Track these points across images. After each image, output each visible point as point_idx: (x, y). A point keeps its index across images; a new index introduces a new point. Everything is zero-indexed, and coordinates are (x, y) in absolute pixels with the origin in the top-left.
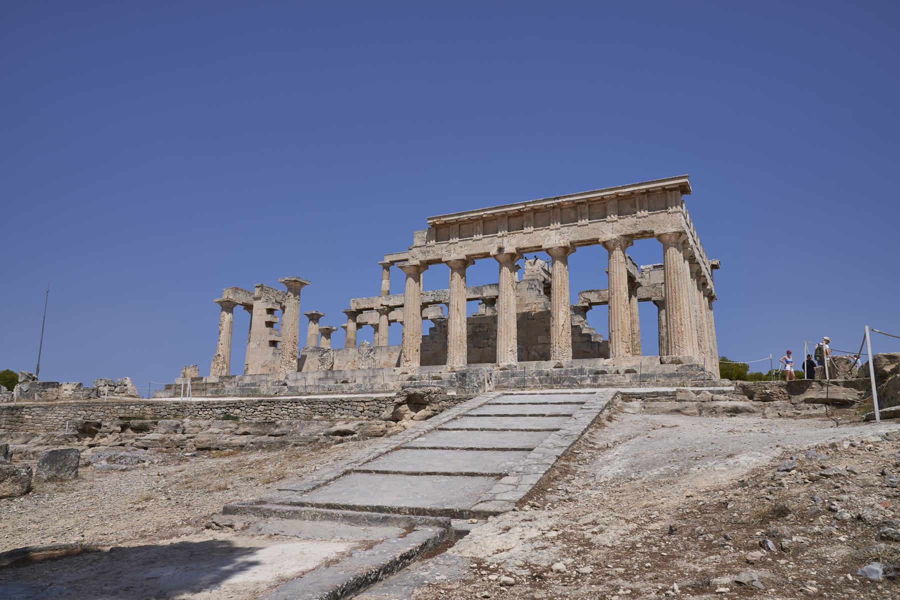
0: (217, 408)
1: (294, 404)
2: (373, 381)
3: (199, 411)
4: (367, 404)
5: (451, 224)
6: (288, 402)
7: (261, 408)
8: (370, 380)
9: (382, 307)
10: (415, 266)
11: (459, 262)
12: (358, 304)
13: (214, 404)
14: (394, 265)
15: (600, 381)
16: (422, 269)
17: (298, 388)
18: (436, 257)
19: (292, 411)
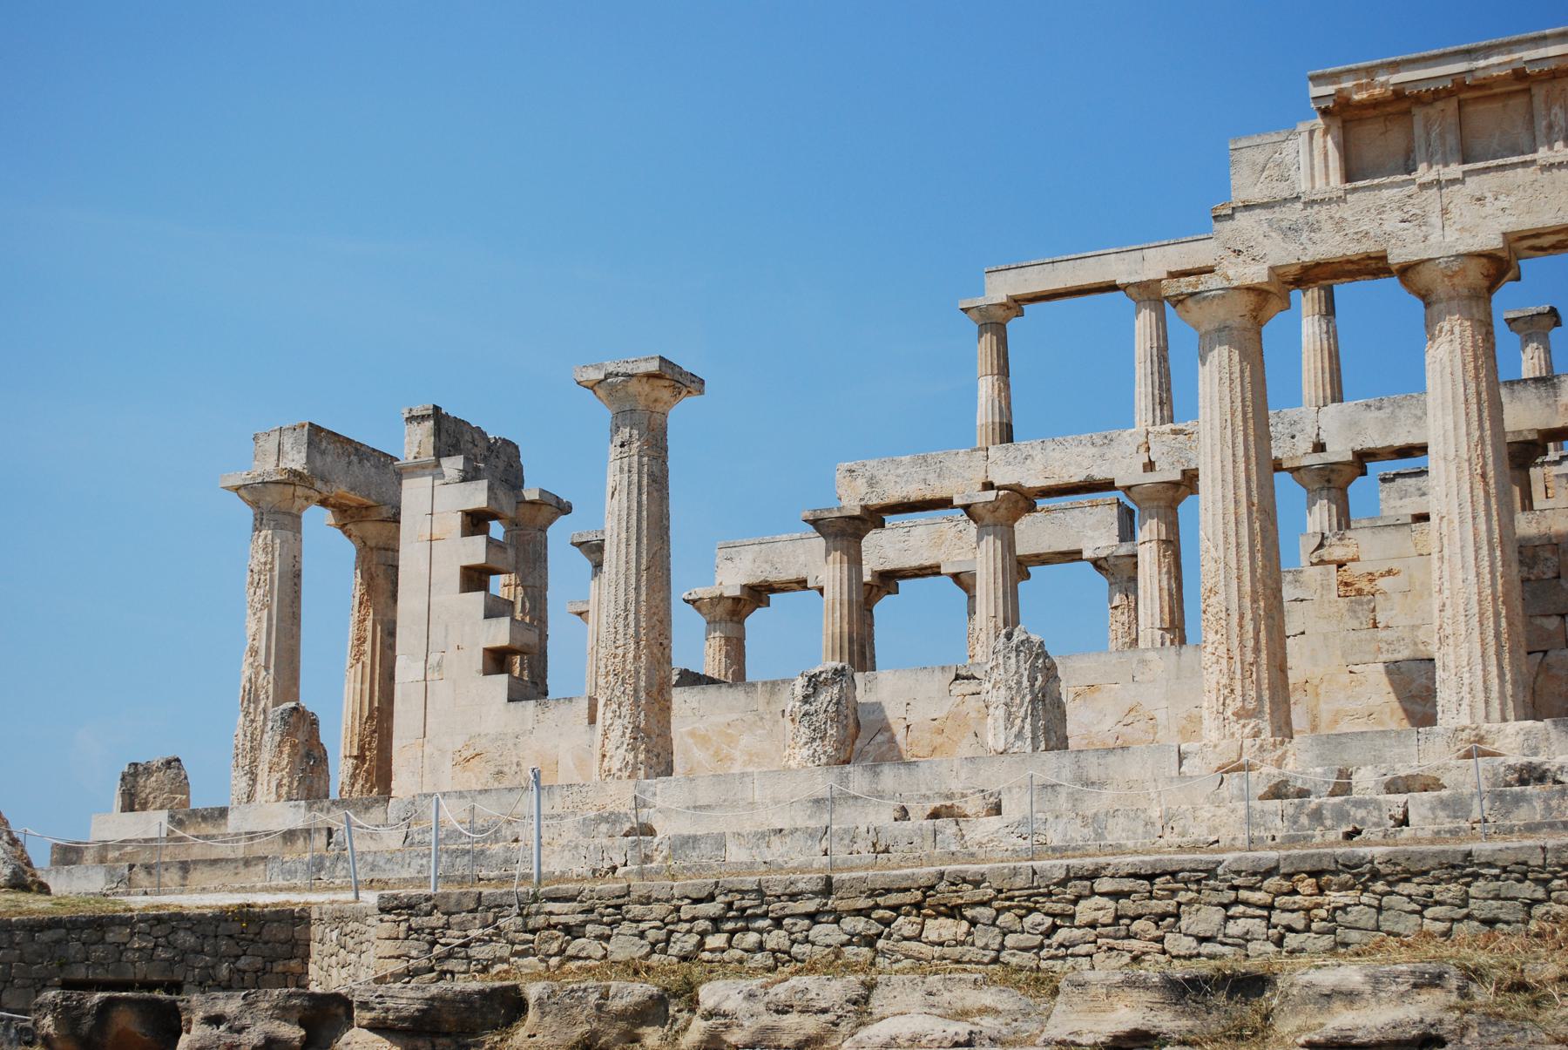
0: (813, 917)
1: (1306, 885)
3: (703, 934)
5: (1419, 100)
6: (1269, 873)
8: (1075, 799)
9: (991, 495)
10: (1249, 289)
11: (1475, 261)
12: (872, 481)
13: (793, 897)
14: (1020, 314)
16: (1274, 303)
17: (720, 842)
18: (1353, 249)
19: (1298, 920)
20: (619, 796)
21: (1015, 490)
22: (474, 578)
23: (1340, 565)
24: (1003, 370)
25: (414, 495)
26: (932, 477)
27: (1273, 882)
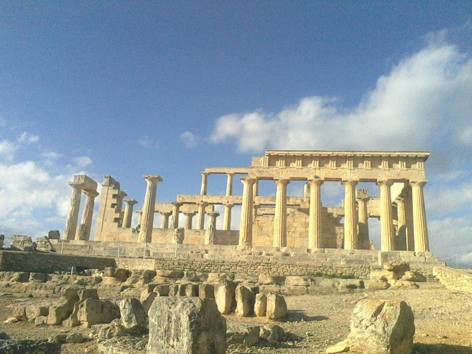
1: (287, 266)
4: (344, 269)
9: (202, 203)
18: (268, 176)
19: (286, 271)
23: (258, 221)
24: (206, 183)
26: (193, 199)
27: (284, 266)
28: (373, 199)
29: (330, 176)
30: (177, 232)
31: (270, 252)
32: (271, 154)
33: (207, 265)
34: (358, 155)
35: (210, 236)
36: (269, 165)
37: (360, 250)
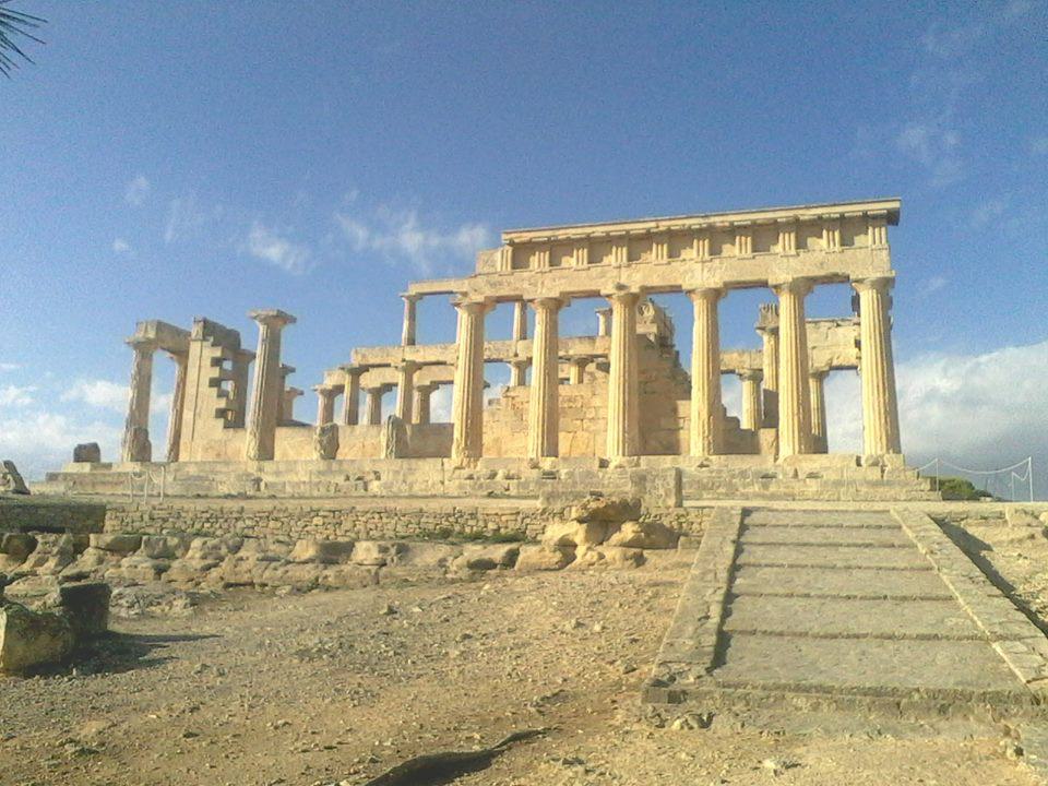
1: (377, 516)
2: (410, 479)
4: (504, 518)
5: (538, 243)
6: (367, 512)
7: (316, 520)
12: (364, 356)
15: (773, 489)
18: (512, 293)
19: (373, 527)
20: (252, 467)
21: (414, 362)
22: (215, 383)
23: (513, 398)
24: (412, 318)
25: (195, 348)
27: (369, 515)
28: (838, 325)
29: (655, 281)
30: (320, 435)
31: (512, 472)
32: (516, 241)
33: (208, 520)
34: (718, 224)
35: (388, 440)
36: (514, 267)
37: (723, 457)
